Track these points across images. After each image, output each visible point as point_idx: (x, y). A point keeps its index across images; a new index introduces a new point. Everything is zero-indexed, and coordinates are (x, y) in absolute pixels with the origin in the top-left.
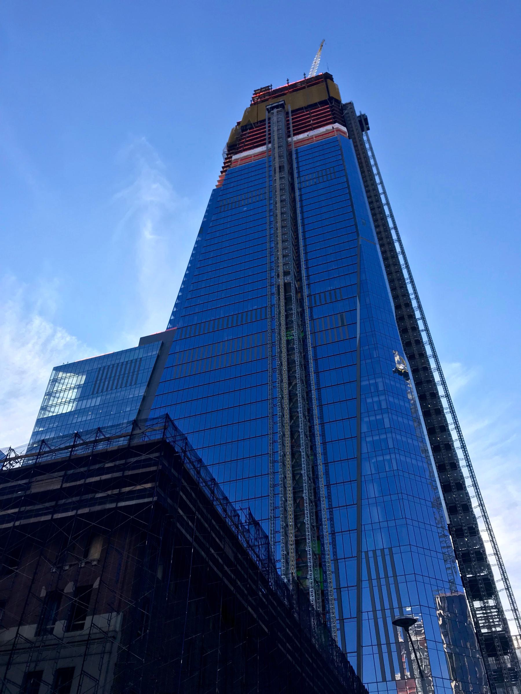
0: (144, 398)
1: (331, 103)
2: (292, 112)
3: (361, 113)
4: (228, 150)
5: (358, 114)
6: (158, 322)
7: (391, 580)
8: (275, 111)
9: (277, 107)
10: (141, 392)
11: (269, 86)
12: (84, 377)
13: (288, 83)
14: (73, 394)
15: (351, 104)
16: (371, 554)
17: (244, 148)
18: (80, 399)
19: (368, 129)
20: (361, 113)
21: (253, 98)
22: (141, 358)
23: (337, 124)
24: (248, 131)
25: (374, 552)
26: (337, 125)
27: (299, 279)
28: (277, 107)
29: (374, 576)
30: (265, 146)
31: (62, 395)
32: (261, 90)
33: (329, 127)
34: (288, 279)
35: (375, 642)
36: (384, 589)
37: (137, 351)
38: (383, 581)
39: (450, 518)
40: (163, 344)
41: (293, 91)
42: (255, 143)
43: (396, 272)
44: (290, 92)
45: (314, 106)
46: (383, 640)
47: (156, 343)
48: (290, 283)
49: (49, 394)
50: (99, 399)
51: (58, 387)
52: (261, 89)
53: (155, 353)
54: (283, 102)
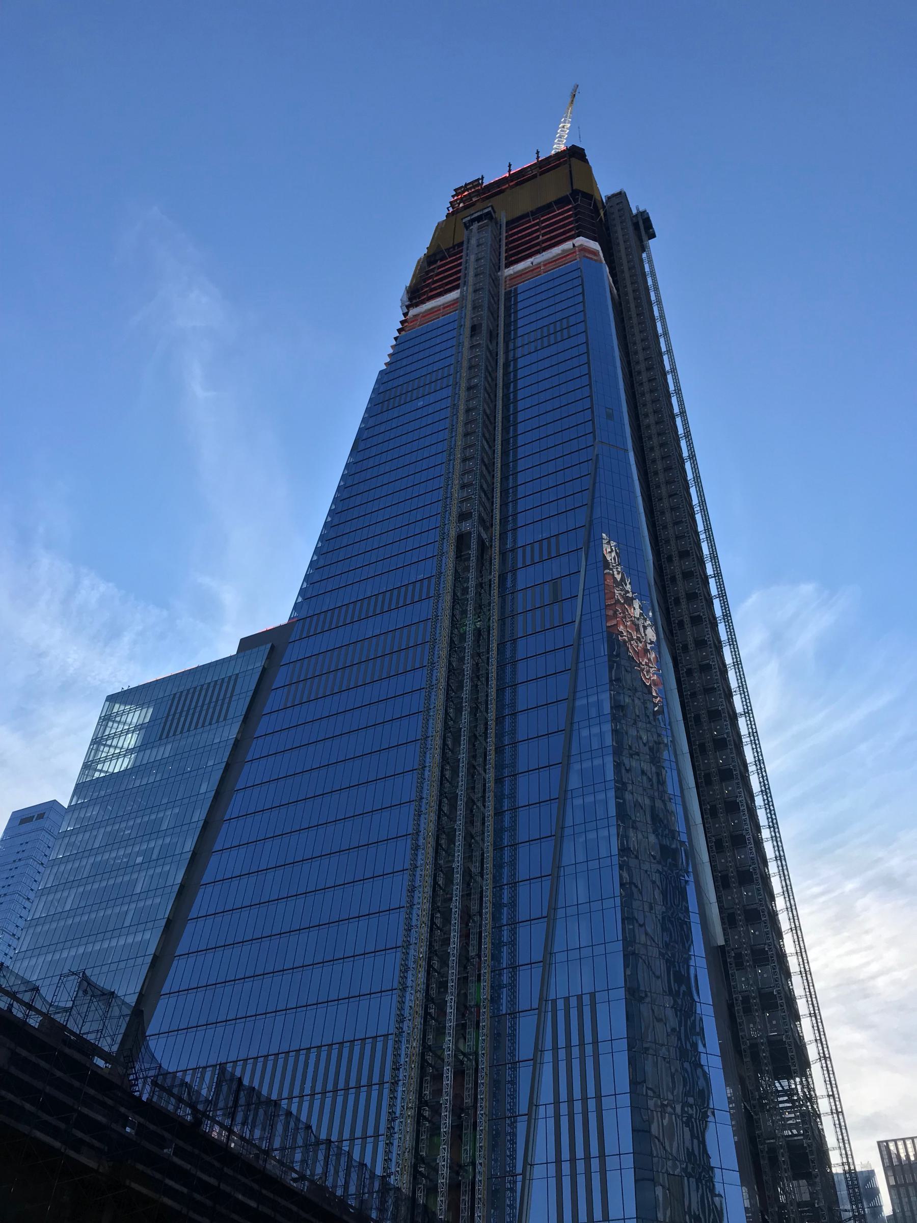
0: (237, 744)
1: (576, 200)
2: (508, 223)
3: (638, 209)
4: (410, 299)
5: (634, 212)
6: (277, 611)
8: (475, 226)
9: (479, 219)
10: (232, 732)
11: (478, 180)
12: (151, 710)
13: (510, 171)
14: (131, 741)
15: (620, 197)
16: (560, 1004)
17: (430, 294)
18: (140, 749)
19: (653, 236)
20: (638, 209)
21: (451, 203)
22: (237, 675)
23: (581, 238)
24: (439, 263)
25: (567, 999)
26: (581, 241)
27: (486, 524)
28: (479, 219)
30: (459, 291)
31: (115, 741)
32: (466, 187)
33: (568, 245)
34: (466, 526)
35: (552, 1157)
36: (576, 1064)
37: (233, 662)
40: (272, 648)
41: (517, 184)
42: (447, 284)
43: (670, 496)
44: (512, 187)
45: (548, 208)
46: (566, 1155)
47: (262, 648)
48: (470, 533)
49: (98, 741)
50: (169, 747)
51: (113, 728)
52: (466, 185)
53: (259, 664)
54: (490, 209)
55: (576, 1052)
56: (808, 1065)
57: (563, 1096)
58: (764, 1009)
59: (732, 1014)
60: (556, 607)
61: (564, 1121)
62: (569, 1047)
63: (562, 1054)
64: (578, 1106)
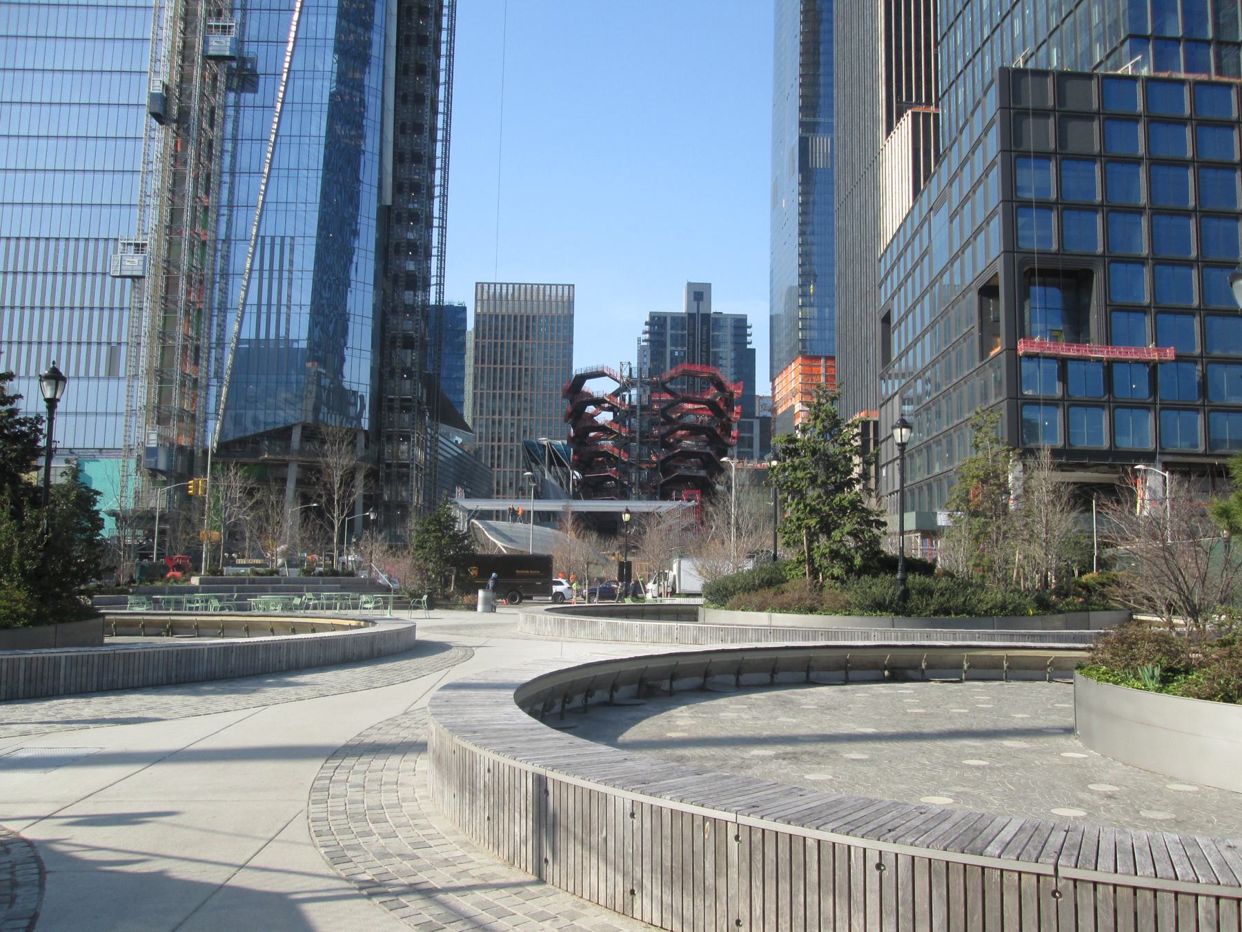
7: (286, 275)
16: (268, 241)
35: (253, 337)
38: (276, 275)
55: (276, 275)
56: (429, 285)
57: (264, 301)
58: (413, 162)
59: (387, 251)
61: (264, 317)
62: (271, 270)
63: (266, 275)
64: (274, 309)
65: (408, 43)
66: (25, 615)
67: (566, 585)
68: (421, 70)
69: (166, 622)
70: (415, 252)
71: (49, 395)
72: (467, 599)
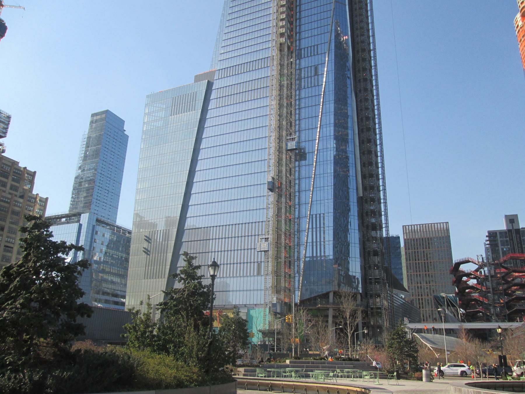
7: (322, 229)
16: (314, 216)
25: (316, 215)
29: (314, 226)
35: (311, 255)
38: (318, 229)
39: (363, 193)
55: (318, 229)
56: (382, 228)
57: (314, 240)
59: (362, 215)
60: (316, 77)
62: (316, 228)
63: (314, 230)
64: (318, 244)
65: (362, 132)
66: (196, 380)
67: (467, 367)
68: (369, 141)
69: (268, 384)
70: (375, 214)
71: (212, 273)
72: (417, 374)
